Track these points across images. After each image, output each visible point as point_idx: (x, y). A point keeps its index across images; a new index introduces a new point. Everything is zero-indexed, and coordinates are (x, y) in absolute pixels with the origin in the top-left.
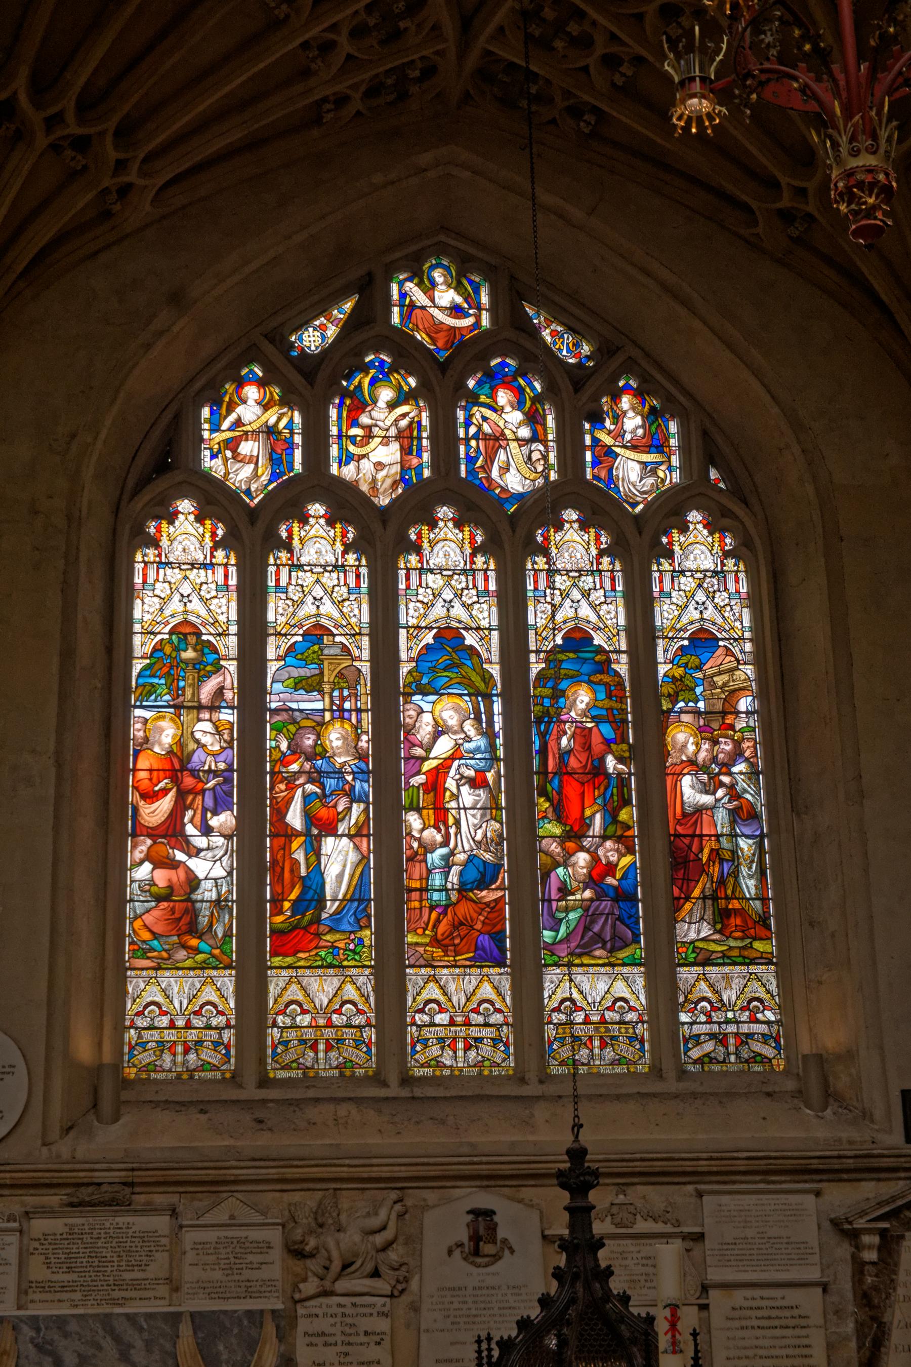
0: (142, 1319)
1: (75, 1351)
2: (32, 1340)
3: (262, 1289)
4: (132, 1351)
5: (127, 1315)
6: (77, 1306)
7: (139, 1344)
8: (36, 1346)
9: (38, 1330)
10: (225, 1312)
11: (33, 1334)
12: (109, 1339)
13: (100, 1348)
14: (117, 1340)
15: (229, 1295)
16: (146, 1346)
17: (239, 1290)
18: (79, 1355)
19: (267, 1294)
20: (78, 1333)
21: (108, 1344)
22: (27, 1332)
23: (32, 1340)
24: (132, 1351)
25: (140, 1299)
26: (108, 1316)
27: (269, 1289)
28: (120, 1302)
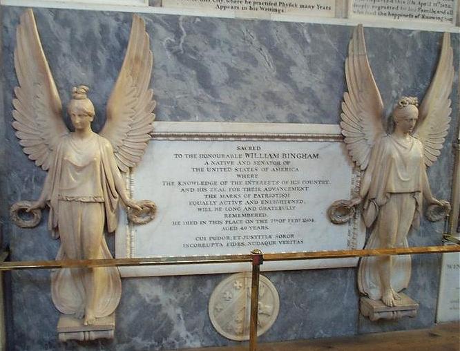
0: (305, 31)
1: (225, 64)
2: (170, 46)
3: (436, 9)
4: (293, 69)
5: (287, 25)
6: (225, 8)
7: (301, 60)
8: (176, 54)
9: (178, 34)
10: (399, 31)
11: (170, 38)
12: (265, 51)
13: (255, 62)
14: (276, 53)
15: (399, 12)
16: (309, 63)
17: (412, 6)
18: (230, 69)
19: (440, 15)
20: (227, 42)
21: (264, 57)
22: (165, 36)
23: (170, 46)
24: (293, 69)
25: (302, 6)
26: (265, 23)
27: (443, 9)
28: (278, 7)
